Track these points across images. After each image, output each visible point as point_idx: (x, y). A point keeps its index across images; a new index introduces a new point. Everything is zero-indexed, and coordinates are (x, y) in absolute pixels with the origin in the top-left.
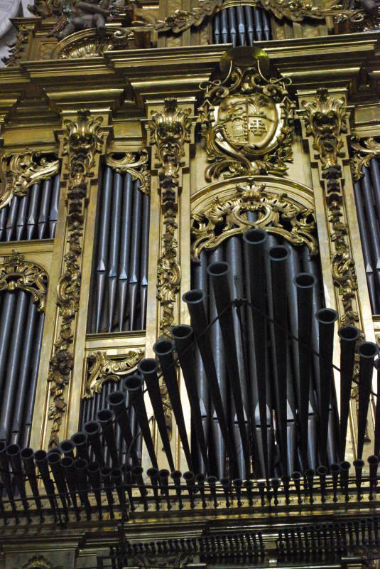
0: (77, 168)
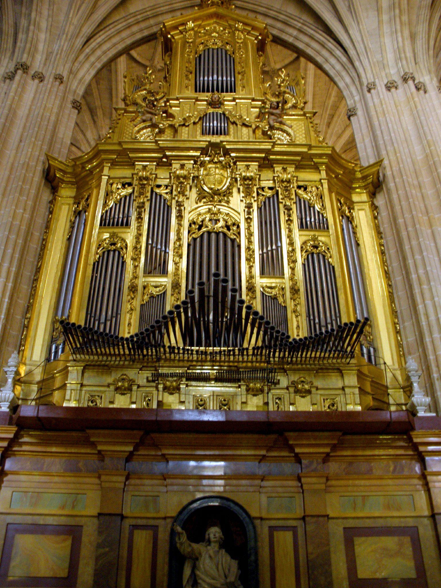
0: (141, 194)
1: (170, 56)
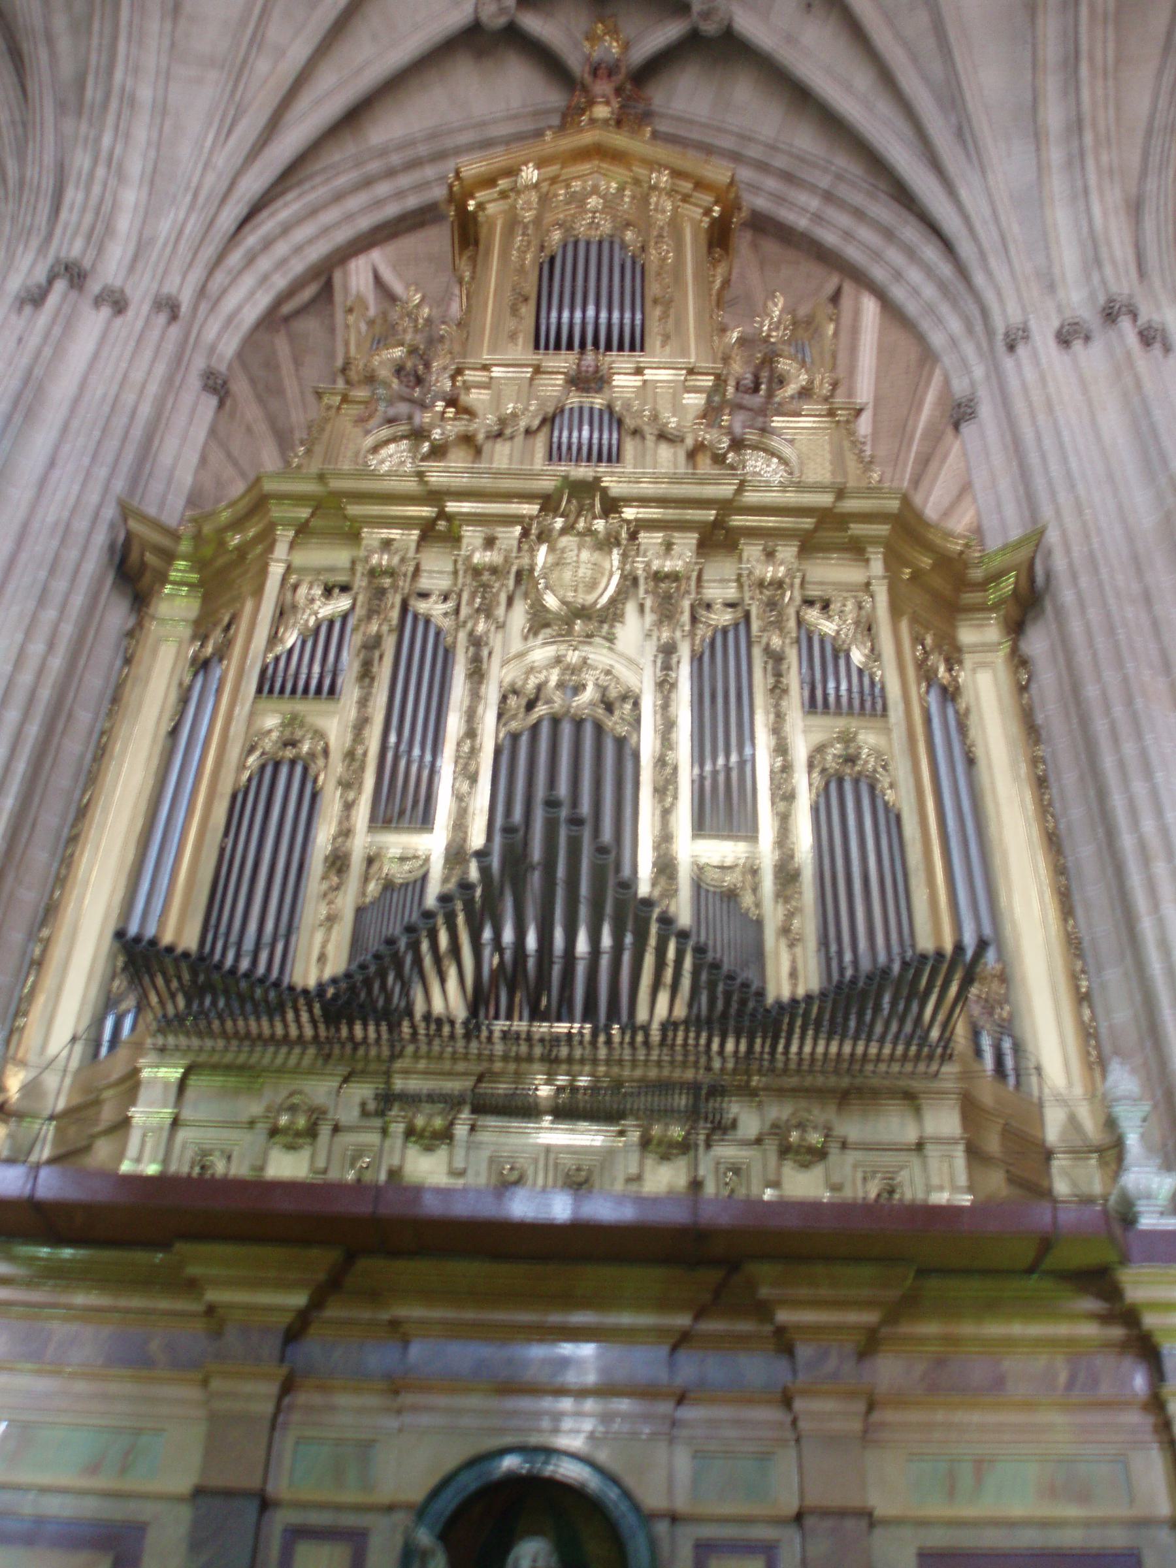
1: (473, 260)
